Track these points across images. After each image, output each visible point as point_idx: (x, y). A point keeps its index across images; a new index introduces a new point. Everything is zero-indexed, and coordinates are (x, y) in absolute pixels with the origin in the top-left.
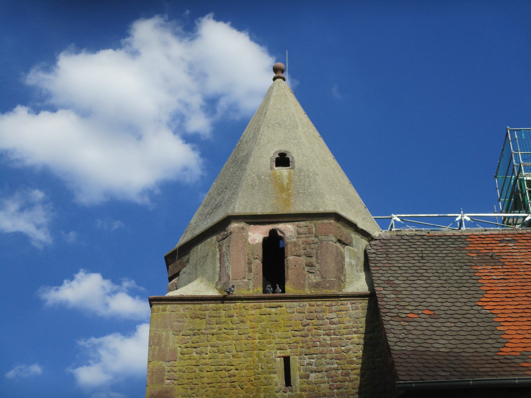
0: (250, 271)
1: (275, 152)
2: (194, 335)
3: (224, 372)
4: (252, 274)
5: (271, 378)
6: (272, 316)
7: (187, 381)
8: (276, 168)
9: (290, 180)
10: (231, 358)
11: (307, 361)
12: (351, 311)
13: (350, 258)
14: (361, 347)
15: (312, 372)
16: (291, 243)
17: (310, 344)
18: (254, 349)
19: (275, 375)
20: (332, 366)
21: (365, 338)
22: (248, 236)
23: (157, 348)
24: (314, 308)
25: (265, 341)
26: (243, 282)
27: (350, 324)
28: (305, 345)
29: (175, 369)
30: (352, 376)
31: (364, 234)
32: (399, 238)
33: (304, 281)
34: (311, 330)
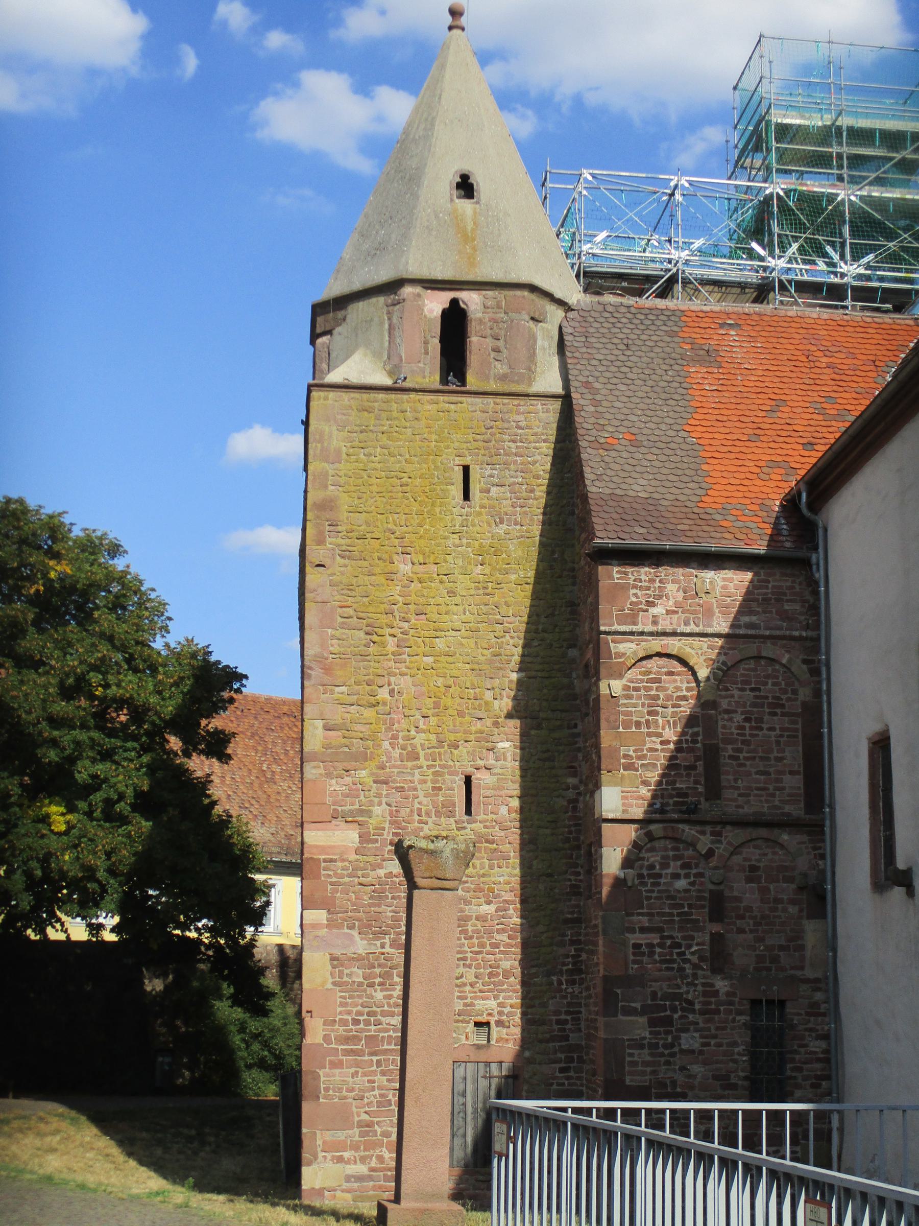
0: (427, 353)
1: (456, 172)
2: (361, 432)
3: (395, 479)
4: (429, 357)
5: (448, 490)
6: (452, 414)
7: (353, 488)
8: (457, 201)
9: (475, 223)
10: (404, 463)
11: (488, 472)
12: (541, 414)
13: (543, 339)
14: (550, 459)
15: (493, 485)
16: (476, 320)
17: (493, 451)
18: (429, 454)
19: (453, 487)
20: (516, 480)
21: (554, 449)
22: (424, 305)
23: (319, 445)
24: (499, 407)
25: (442, 445)
26: (419, 367)
27: (540, 430)
28: (487, 452)
29: (341, 473)
30: (538, 494)
31: (560, 303)
33: (489, 371)
34: (495, 434)
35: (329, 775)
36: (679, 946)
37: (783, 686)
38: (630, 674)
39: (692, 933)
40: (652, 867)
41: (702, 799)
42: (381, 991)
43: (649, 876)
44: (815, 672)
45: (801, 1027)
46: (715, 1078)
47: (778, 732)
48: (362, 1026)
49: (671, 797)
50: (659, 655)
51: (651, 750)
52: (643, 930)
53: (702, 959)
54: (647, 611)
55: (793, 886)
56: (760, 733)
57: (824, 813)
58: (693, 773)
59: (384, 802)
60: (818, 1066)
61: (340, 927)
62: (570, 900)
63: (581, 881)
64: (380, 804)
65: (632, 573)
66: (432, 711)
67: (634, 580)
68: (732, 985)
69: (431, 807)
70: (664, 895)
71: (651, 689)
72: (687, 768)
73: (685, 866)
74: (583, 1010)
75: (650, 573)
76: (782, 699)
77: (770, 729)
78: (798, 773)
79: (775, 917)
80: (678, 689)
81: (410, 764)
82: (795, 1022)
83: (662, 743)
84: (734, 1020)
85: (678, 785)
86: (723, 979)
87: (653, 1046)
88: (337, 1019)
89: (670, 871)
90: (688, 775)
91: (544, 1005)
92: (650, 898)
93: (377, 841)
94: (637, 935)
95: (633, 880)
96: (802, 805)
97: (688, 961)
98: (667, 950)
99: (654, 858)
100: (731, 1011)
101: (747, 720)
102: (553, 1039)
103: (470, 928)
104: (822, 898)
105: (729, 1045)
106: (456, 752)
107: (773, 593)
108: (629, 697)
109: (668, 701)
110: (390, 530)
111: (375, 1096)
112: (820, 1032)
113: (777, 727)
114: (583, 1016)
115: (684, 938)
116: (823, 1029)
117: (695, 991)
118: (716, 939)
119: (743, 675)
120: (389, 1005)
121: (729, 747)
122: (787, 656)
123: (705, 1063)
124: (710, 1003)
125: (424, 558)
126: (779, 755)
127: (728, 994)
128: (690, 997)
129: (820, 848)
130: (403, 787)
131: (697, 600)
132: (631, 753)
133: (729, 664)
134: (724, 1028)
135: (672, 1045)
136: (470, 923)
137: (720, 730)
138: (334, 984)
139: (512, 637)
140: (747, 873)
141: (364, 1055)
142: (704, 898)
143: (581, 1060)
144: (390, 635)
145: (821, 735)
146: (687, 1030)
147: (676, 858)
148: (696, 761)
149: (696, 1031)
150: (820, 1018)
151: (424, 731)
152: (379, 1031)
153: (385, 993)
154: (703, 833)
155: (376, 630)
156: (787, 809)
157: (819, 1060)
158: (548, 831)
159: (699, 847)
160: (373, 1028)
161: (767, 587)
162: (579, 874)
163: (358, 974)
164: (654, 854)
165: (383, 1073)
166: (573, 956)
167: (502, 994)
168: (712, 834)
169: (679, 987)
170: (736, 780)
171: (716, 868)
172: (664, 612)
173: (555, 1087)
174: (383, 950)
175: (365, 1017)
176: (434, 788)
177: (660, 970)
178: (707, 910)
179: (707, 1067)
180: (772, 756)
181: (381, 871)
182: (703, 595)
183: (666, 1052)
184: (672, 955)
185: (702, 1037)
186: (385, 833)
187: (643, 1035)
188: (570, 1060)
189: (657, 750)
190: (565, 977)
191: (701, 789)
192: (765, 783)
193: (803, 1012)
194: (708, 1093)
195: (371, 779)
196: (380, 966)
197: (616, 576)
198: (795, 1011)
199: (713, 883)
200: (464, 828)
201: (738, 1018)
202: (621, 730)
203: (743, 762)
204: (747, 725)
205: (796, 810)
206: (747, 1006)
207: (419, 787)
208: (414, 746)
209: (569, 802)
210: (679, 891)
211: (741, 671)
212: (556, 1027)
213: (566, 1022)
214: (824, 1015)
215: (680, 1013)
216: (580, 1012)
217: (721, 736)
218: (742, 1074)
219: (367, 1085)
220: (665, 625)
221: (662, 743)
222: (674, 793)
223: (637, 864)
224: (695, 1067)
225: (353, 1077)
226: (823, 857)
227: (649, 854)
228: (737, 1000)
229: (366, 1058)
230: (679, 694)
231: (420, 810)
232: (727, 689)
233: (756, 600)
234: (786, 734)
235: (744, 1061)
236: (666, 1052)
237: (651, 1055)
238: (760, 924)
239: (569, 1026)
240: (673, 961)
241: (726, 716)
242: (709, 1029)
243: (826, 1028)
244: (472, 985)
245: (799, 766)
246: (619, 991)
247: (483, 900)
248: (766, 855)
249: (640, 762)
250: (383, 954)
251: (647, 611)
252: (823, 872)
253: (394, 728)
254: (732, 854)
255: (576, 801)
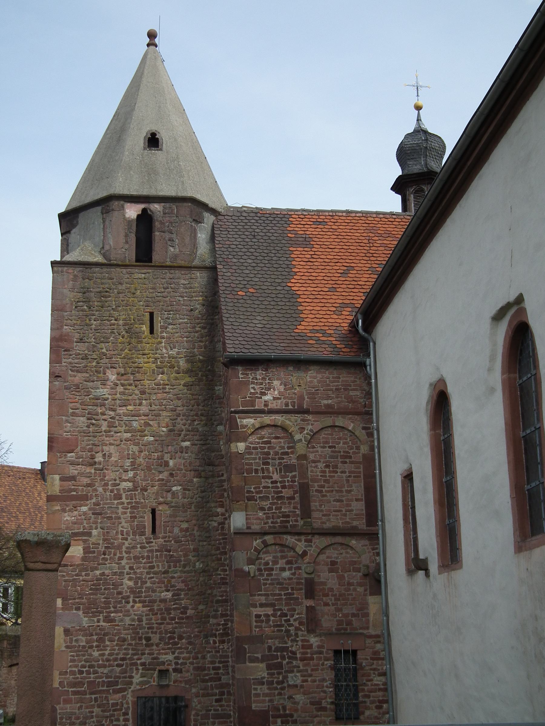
15: (169, 324)
20: (184, 321)
22: (126, 213)
32: (239, 214)
34: (170, 292)
35: (64, 511)
36: (286, 615)
37: (350, 444)
38: (251, 439)
39: (294, 607)
40: (267, 564)
41: (299, 519)
42: (98, 651)
43: (266, 570)
44: (370, 435)
45: (367, 668)
46: (312, 703)
47: (347, 474)
48: (84, 675)
49: (279, 517)
50: (268, 426)
51: (264, 487)
52: (262, 605)
53: (301, 623)
54: (261, 398)
55: (360, 574)
56: (336, 475)
57: (378, 525)
58: (292, 501)
59: (99, 527)
60: (381, 693)
61: (71, 609)
62: (220, 588)
63: (227, 575)
64: (96, 528)
65: (251, 374)
66: (129, 468)
67: (252, 379)
68: (321, 640)
69: (129, 529)
70: (275, 582)
71: (264, 448)
72: (289, 498)
73: (289, 562)
74: (230, 660)
75: (263, 374)
76: (350, 453)
77: (342, 472)
78: (361, 500)
79: (349, 595)
80: (283, 448)
81: (116, 502)
82: (364, 664)
83: (272, 482)
84: (323, 664)
85: (283, 510)
86: (315, 637)
87: (270, 683)
88: (68, 671)
89: (278, 566)
90: (290, 503)
91: (204, 657)
92: (266, 584)
93: (94, 552)
94: (259, 609)
95: (255, 572)
96: (364, 521)
97: (292, 625)
98: (278, 618)
99: (269, 558)
100: (321, 658)
101: (327, 466)
102: (211, 680)
103: (155, 608)
104: (379, 581)
105: (320, 681)
106: (145, 493)
107: (342, 385)
108: (251, 453)
109: (276, 455)
110: (103, 353)
111: (93, 722)
112: (381, 671)
113: (347, 470)
114: (230, 664)
115: (288, 610)
116: (382, 669)
117: (297, 645)
118: (310, 610)
119: (323, 438)
120: (103, 661)
121: (316, 484)
122: (352, 425)
123: (304, 694)
124: (307, 653)
125: (125, 370)
126: (349, 489)
127: (319, 647)
128: (294, 649)
129: (377, 548)
130: (111, 517)
131: (293, 390)
132: (252, 489)
133: (315, 431)
134: (317, 670)
135: (282, 682)
136: (156, 604)
137: (309, 473)
138: (67, 647)
139: (182, 420)
140: (329, 566)
141: (86, 695)
142: (301, 583)
143: (229, 693)
144: (103, 420)
145: (374, 476)
146: (292, 672)
147: (283, 557)
148: (294, 494)
149: (298, 672)
150: (380, 662)
151: (125, 481)
152: (97, 678)
153: (100, 652)
154: (300, 540)
155: (94, 417)
156: (355, 523)
157: (380, 690)
158: (205, 543)
159: (297, 549)
160: (92, 676)
161: (339, 382)
162: (226, 570)
163: (83, 641)
164: (268, 555)
165: (99, 706)
166: (223, 624)
167: (178, 651)
168: (306, 541)
169: (286, 643)
170: (321, 506)
171: (309, 563)
172: (272, 398)
173: (212, 712)
174: (99, 624)
175: (87, 669)
176: (131, 517)
177: (274, 632)
178: (303, 591)
179: (306, 696)
180: (344, 489)
181: (97, 572)
182: (297, 387)
183: (279, 687)
184: (281, 621)
185: (302, 676)
186: (100, 547)
187: (263, 675)
188: (222, 694)
189: (269, 487)
190: (218, 638)
191: (298, 512)
192: (340, 507)
193: (369, 658)
194: (307, 714)
195: (91, 512)
196: (96, 634)
197: (241, 376)
198: (364, 657)
199: (307, 573)
200: (152, 542)
201: (326, 663)
202: (245, 475)
203: (324, 494)
204: (327, 470)
205: (361, 524)
206: (331, 654)
207: (122, 516)
208: (118, 490)
209: (220, 524)
210: (285, 579)
211: (322, 436)
212: (212, 672)
213: (219, 668)
214: (383, 659)
215: (287, 660)
216: (228, 662)
217: (310, 477)
218: (329, 700)
219: (88, 714)
220: (273, 405)
221: (272, 482)
222: (281, 515)
223: (257, 562)
224: (298, 696)
225: (79, 710)
226: (378, 554)
227: (265, 555)
228: (325, 650)
229: (88, 696)
230: (282, 451)
231: (122, 531)
232: (314, 447)
233: (332, 390)
234: (353, 475)
235: (331, 692)
236: (279, 687)
237: (268, 689)
238: (339, 600)
239: (221, 671)
240: (282, 626)
241: (313, 465)
242: (307, 671)
243: (385, 668)
244: (157, 645)
245: (362, 496)
246: (246, 647)
247: (164, 589)
248: (342, 554)
249: (258, 496)
250: (98, 626)
251: (261, 398)
252: (378, 564)
253: (106, 478)
254: (319, 554)
255: (223, 523)
